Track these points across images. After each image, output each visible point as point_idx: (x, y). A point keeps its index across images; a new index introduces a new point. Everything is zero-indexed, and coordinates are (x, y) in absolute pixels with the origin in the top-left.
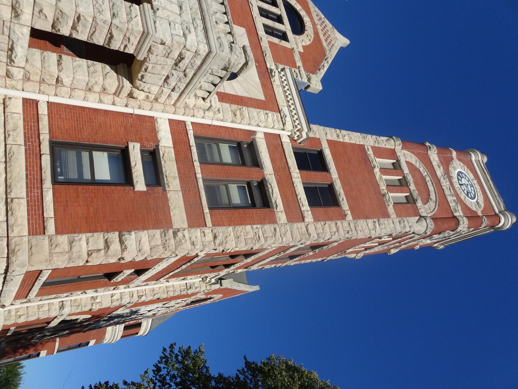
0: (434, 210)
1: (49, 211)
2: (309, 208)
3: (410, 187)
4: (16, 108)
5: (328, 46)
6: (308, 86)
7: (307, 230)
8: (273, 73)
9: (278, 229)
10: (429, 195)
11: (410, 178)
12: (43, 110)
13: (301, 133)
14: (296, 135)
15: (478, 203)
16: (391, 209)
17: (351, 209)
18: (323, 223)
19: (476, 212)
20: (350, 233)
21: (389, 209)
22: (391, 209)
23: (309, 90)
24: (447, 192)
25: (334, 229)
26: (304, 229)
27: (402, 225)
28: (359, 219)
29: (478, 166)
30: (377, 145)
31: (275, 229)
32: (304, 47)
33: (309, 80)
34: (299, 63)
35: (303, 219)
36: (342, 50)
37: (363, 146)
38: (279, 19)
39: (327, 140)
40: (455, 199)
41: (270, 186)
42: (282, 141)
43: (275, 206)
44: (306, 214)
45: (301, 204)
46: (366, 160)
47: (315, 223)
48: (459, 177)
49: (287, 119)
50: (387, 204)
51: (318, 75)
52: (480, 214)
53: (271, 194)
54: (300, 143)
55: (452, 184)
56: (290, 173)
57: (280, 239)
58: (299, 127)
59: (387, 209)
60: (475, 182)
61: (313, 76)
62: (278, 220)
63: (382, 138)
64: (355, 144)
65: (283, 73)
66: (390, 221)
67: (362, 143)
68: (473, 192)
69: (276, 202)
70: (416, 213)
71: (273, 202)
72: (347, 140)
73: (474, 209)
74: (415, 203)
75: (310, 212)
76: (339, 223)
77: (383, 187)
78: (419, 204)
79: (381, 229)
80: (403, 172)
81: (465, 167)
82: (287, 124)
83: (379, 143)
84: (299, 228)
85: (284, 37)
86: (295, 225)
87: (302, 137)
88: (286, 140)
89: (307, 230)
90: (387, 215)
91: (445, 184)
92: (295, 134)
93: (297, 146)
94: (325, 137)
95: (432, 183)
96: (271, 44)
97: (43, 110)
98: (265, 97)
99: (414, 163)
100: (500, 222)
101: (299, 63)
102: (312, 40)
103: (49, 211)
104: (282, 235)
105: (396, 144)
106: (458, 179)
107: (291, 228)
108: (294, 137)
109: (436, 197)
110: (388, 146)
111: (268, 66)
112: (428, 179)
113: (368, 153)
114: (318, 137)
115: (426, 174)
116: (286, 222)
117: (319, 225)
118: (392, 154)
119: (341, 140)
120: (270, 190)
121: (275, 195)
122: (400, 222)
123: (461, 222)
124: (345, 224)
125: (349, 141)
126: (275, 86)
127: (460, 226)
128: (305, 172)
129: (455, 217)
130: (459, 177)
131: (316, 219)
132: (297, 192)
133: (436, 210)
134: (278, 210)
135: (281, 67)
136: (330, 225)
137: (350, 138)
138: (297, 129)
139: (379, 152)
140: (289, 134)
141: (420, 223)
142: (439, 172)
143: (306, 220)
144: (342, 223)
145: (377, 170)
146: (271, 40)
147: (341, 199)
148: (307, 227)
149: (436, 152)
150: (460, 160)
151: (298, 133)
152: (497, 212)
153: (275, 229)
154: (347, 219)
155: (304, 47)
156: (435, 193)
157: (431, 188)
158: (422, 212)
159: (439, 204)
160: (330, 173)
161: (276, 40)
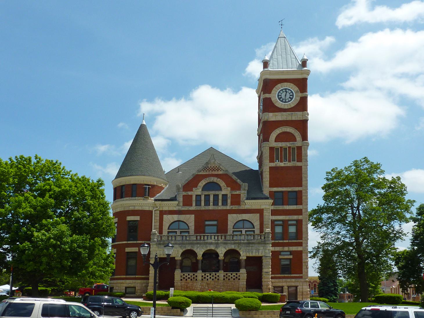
1: (298, 275)
4: (273, 280)
5: (221, 171)
12: (273, 275)
28: (302, 184)
35: (302, 210)
40: (293, 113)
44: (300, 208)
72: (268, 176)
76: (303, 194)
88: (273, 208)
97: (273, 275)
98: (258, 213)
101: (238, 192)
103: (298, 275)
133: (300, 134)
159: (296, 129)
161: (229, 201)
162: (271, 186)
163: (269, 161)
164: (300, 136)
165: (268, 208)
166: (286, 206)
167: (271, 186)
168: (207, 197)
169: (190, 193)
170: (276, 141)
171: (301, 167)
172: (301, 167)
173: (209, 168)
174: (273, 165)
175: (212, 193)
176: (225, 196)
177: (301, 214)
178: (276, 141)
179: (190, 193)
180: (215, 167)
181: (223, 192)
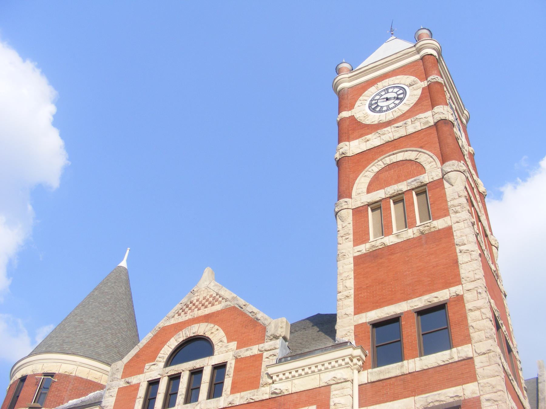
0: (432, 157)
2: (454, 350)
3: (404, 190)
6: (285, 338)
7: (484, 354)
8: (277, 391)
9: (488, 396)
10: (411, 160)
11: (392, 190)
13: (354, 357)
14: (357, 362)
15: (411, 85)
16: (440, 224)
17: (447, 285)
18: (471, 330)
19: (423, 89)
20: (479, 291)
21: (440, 227)
22: (440, 224)
23: (288, 337)
24: (402, 132)
25: (477, 313)
26: (483, 358)
27: (458, 208)
28: (459, 275)
29: (357, 79)
30: (351, 237)
31: (488, 400)
32: (230, 340)
33: (276, 338)
34: (254, 350)
36: (219, 278)
37: (355, 258)
38: (197, 373)
39: (355, 314)
40: (409, 120)
41: (431, 405)
42: (366, 382)
43: (457, 399)
44: (463, 355)
45: (451, 361)
46: (374, 255)
47: (473, 341)
48: (378, 109)
49: (338, 377)
50: (433, 230)
51: (266, 323)
52: (425, 84)
53: (442, 403)
54: (366, 356)
55: (388, 123)
56: (409, 373)
57: (499, 393)
58: (347, 360)
59: (439, 230)
60: (382, 85)
61: (271, 330)
62: (475, 396)
63: (340, 227)
64: (355, 271)
65: (275, 377)
66: (455, 227)
67: (352, 260)
68: (396, 90)
69: (451, 397)
70: (439, 184)
71: (451, 400)
72: (350, 283)
73: (419, 92)
74: (426, 185)
75: (459, 348)
76: (468, 306)
77: (410, 233)
78: (426, 178)
79: (470, 243)
80: (383, 199)
81: (361, 98)
82: (345, 377)
83: (348, 234)
84: (482, 365)
85: (220, 368)
86: (479, 371)
87: (360, 356)
88: (365, 377)
89: (484, 354)
90: (448, 231)
91: (390, 134)
92: (356, 364)
93: (370, 361)
94: (352, 317)
95: (394, 154)
96: (235, 389)
99: (368, 180)
100: (431, 55)
101: (254, 350)
102: (216, 327)
104: (495, 390)
105: (346, 207)
106: (380, 111)
107: (484, 377)
108: (360, 366)
109: (412, 151)
110: (350, 219)
111: (267, 396)
112: (388, 161)
113: (364, 251)
114: (353, 328)
115: (380, 163)
116: (476, 383)
117: (475, 335)
118: (359, 213)
119: (352, 292)
120: (437, 404)
121: (442, 398)
122: (456, 212)
123: (443, 117)
124: (468, 296)
125: (352, 280)
126: (294, 390)
127: (447, 118)
128: (406, 352)
129: (436, 124)
130: (378, 109)
131: (467, 340)
132: (436, 365)
133: (431, 154)
134: (461, 394)
135: (265, 379)
136: (475, 321)
137: (347, 277)
138: (350, 362)
139: (361, 236)
140: (356, 372)
141: (452, 181)
142: (374, 140)
143: (470, 355)
144: (468, 302)
145: (390, 240)
146: (229, 389)
147: (436, 300)
148: (479, 354)
149: (347, 143)
150: (352, 107)
151: (355, 361)
152: (418, 57)
153: (488, 400)
154: (461, 293)
155: (230, 340)
156: (407, 151)
157: (400, 157)
158: (437, 175)
159: (421, 147)
160: (402, 313)
161: (228, 382)
162: (359, 309)
163: (352, 242)
164: (434, 157)
165: (347, 376)
166: (410, 361)
167: (359, 309)
168: (175, 379)
169: (134, 380)
170: (369, 190)
171: (450, 228)
172: (450, 228)
173: (194, 305)
174: (364, 248)
175: (184, 368)
176: (220, 368)
177: (472, 377)
178: (369, 190)
179: (134, 380)
180: (208, 297)
181: (216, 360)
